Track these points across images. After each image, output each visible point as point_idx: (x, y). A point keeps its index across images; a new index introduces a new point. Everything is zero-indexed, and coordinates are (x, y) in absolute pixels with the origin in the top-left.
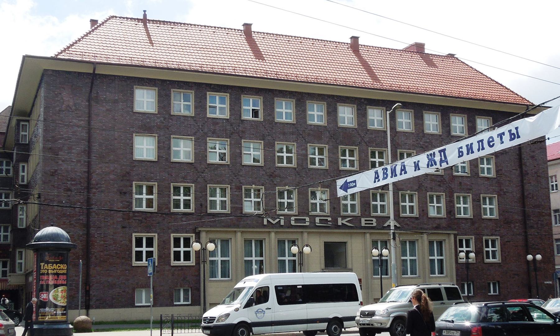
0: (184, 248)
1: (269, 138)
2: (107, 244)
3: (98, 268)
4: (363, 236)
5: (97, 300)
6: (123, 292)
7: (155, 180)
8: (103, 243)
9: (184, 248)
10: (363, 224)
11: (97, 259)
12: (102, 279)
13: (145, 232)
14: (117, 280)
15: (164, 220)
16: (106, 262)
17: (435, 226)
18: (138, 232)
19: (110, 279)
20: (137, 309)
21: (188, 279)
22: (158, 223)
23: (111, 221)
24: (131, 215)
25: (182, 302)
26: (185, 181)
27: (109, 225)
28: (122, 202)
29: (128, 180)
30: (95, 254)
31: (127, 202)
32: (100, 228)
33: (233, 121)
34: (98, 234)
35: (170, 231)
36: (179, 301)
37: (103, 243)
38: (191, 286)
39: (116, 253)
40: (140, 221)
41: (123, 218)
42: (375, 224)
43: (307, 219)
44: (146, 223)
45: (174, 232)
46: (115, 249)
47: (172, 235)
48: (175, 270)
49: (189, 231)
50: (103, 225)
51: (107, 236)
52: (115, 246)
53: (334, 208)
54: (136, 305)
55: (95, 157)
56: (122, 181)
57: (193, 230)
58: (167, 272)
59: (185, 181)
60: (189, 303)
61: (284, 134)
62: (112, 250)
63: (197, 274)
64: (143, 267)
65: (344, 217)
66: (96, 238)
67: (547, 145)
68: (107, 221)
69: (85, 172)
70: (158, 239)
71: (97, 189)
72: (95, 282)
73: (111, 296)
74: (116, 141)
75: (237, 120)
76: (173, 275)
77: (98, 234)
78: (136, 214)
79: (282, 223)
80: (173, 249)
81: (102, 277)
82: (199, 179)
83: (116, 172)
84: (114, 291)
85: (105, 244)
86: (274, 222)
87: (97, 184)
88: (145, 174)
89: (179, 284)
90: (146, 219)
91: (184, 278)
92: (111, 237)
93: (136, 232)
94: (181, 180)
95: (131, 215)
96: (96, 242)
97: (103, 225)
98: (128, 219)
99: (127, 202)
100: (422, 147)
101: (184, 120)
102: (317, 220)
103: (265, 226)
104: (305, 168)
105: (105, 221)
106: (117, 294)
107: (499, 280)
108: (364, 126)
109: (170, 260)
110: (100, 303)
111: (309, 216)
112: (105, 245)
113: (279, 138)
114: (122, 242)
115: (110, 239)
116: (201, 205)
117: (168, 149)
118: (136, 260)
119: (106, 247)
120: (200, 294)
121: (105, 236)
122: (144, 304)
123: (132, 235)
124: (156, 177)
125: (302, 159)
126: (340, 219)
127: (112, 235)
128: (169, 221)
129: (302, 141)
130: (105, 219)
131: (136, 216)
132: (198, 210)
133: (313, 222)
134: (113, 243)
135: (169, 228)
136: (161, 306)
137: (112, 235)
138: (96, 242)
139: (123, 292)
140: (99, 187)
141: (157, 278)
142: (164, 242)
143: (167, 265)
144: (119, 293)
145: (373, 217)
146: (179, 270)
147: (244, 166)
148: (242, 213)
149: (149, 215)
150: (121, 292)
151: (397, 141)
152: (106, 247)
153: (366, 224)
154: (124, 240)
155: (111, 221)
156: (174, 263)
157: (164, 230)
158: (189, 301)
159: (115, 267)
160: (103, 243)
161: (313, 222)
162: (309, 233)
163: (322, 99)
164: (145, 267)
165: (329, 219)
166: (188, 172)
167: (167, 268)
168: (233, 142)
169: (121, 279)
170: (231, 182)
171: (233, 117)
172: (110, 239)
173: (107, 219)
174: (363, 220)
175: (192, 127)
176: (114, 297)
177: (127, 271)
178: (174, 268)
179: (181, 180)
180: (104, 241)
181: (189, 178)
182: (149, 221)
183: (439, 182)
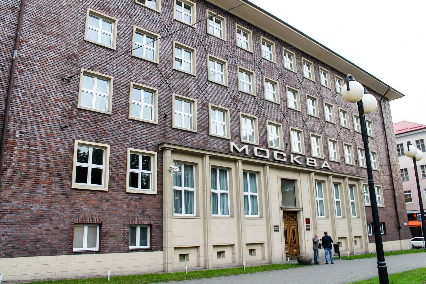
0: (142, 169)
1: (231, 60)
2: (34, 150)
3: (16, 188)
4: (308, 175)
5: (9, 242)
6: (55, 228)
7: (111, 73)
8: (27, 147)
9: (142, 169)
10: (308, 164)
11: (14, 172)
12: (20, 207)
13: (94, 140)
14: (47, 209)
15: (119, 127)
16: (31, 178)
17: (349, 172)
18: (83, 139)
19: (35, 207)
20: (76, 256)
21: (147, 213)
22: (112, 131)
23: (45, 117)
24: (75, 112)
25: (138, 246)
26: (148, 83)
27: (40, 122)
28: (63, 92)
29: (74, 65)
30: (13, 164)
31: (72, 94)
32: (26, 123)
33: (199, 33)
34: (21, 132)
35: (127, 144)
36: (135, 245)
37: (27, 147)
38: (152, 223)
39: (48, 166)
40: (87, 123)
41: (63, 116)
42: (315, 165)
43: (268, 151)
44: (95, 128)
45: (131, 146)
46: (46, 160)
47: (129, 149)
48: (131, 199)
49: (150, 147)
50: (30, 120)
51: (35, 139)
52: (47, 156)
53: (286, 145)
54: (75, 249)
55: (28, 20)
56: (66, 63)
57: (155, 147)
58: (121, 202)
59: (148, 83)
60: (148, 247)
61: (244, 60)
62: (42, 161)
63: (159, 206)
64: (88, 192)
65: (295, 154)
66: (17, 138)
67: (394, 122)
68: (38, 116)
69: (9, 37)
70: (111, 153)
71: (26, 66)
72: (9, 211)
73: (34, 234)
74: (63, 11)
75: (203, 32)
76: (128, 207)
77: (21, 132)
78: (83, 114)
79: (247, 153)
80: (130, 170)
81: (21, 203)
82: (163, 85)
83: (58, 49)
84: (39, 228)
85: (32, 150)
86: (240, 150)
87: (28, 59)
88: (98, 63)
89: (136, 219)
90: (95, 123)
91: (143, 212)
92: (42, 140)
93: (79, 138)
94: (143, 81)
95: (75, 112)
96: (16, 145)
97: (30, 120)
98: (69, 118)
99: (72, 94)
100: (336, 103)
101: (149, 13)
102: (275, 153)
103: (230, 153)
104: (262, 99)
105: (34, 116)
106: (44, 232)
107: (383, 222)
108: (301, 74)
109: (126, 184)
110: (13, 248)
111: (269, 149)
112: (31, 152)
113: (240, 62)
114: (57, 150)
115: (41, 143)
116: (165, 116)
117: (129, 41)
118: (77, 181)
119: (33, 154)
120: (162, 234)
121: (31, 138)
122: (85, 248)
123: (74, 143)
124: (113, 70)
125: (260, 90)
126: (292, 156)
127: (44, 138)
128: (126, 130)
129: (259, 72)
130: (34, 111)
131: (81, 116)
132: (161, 122)
133: (272, 155)
134: (45, 150)
135: (125, 140)
136: (112, 251)
137: (44, 138)
138: (16, 145)
139: (55, 228)
140: (30, 64)
141: (107, 210)
142: (118, 157)
143: (120, 191)
144: (49, 230)
145: (313, 158)
146: (136, 199)
147: (209, 81)
148: (208, 134)
149: (100, 117)
150: (50, 228)
151: (322, 93)
152: (33, 154)
153: (310, 163)
154: (62, 148)
155: (45, 117)
156: (130, 189)
157: (118, 141)
158: (147, 245)
159: (44, 187)
160: (28, 147)
161: (272, 155)
162: (272, 167)
163: (271, 39)
164: (90, 192)
165: (285, 154)
166: (152, 74)
167: (121, 195)
168: (199, 54)
169: (52, 208)
170: (197, 96)
171: (199, 28)
172: (41, 143)
173: (37, 112)
174: (308, 159)
175: (158, 24)
176: (40, 236)
177: (63, 196)
178: (129, 197)
179: (143, 81)
180: (30, 145)
181: (152, 80)
182: (100, 126)
183: (348, 135)
